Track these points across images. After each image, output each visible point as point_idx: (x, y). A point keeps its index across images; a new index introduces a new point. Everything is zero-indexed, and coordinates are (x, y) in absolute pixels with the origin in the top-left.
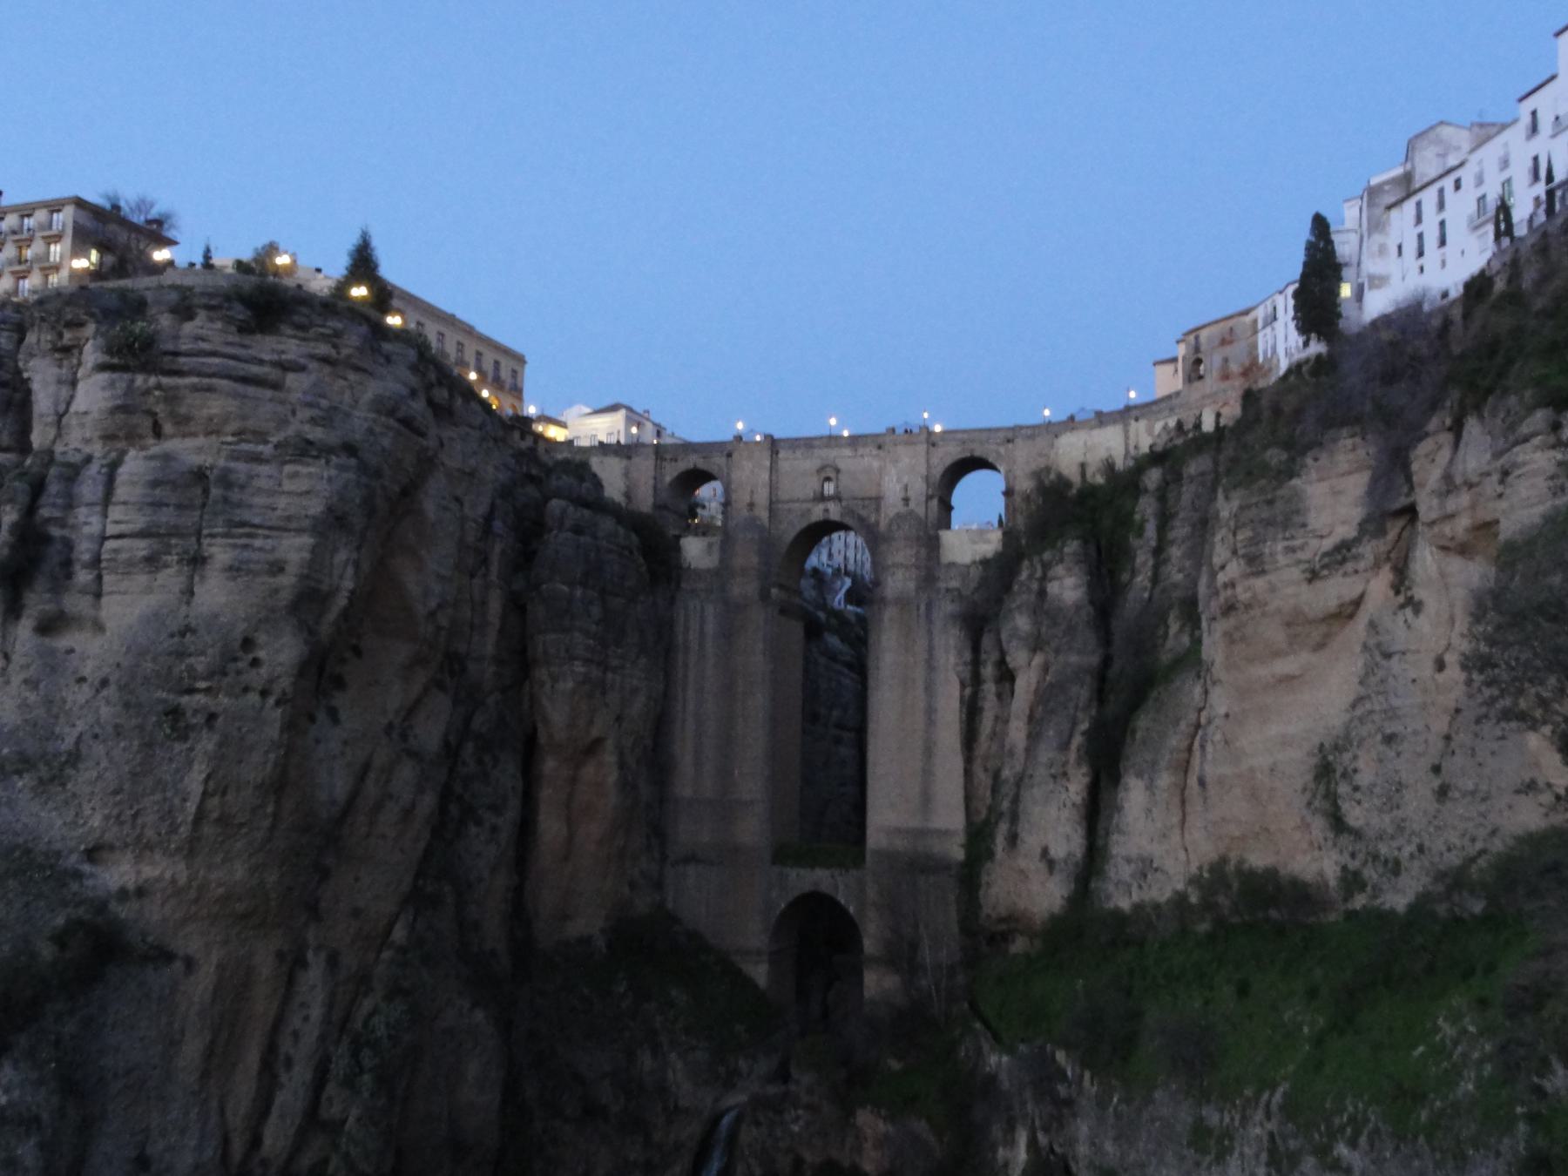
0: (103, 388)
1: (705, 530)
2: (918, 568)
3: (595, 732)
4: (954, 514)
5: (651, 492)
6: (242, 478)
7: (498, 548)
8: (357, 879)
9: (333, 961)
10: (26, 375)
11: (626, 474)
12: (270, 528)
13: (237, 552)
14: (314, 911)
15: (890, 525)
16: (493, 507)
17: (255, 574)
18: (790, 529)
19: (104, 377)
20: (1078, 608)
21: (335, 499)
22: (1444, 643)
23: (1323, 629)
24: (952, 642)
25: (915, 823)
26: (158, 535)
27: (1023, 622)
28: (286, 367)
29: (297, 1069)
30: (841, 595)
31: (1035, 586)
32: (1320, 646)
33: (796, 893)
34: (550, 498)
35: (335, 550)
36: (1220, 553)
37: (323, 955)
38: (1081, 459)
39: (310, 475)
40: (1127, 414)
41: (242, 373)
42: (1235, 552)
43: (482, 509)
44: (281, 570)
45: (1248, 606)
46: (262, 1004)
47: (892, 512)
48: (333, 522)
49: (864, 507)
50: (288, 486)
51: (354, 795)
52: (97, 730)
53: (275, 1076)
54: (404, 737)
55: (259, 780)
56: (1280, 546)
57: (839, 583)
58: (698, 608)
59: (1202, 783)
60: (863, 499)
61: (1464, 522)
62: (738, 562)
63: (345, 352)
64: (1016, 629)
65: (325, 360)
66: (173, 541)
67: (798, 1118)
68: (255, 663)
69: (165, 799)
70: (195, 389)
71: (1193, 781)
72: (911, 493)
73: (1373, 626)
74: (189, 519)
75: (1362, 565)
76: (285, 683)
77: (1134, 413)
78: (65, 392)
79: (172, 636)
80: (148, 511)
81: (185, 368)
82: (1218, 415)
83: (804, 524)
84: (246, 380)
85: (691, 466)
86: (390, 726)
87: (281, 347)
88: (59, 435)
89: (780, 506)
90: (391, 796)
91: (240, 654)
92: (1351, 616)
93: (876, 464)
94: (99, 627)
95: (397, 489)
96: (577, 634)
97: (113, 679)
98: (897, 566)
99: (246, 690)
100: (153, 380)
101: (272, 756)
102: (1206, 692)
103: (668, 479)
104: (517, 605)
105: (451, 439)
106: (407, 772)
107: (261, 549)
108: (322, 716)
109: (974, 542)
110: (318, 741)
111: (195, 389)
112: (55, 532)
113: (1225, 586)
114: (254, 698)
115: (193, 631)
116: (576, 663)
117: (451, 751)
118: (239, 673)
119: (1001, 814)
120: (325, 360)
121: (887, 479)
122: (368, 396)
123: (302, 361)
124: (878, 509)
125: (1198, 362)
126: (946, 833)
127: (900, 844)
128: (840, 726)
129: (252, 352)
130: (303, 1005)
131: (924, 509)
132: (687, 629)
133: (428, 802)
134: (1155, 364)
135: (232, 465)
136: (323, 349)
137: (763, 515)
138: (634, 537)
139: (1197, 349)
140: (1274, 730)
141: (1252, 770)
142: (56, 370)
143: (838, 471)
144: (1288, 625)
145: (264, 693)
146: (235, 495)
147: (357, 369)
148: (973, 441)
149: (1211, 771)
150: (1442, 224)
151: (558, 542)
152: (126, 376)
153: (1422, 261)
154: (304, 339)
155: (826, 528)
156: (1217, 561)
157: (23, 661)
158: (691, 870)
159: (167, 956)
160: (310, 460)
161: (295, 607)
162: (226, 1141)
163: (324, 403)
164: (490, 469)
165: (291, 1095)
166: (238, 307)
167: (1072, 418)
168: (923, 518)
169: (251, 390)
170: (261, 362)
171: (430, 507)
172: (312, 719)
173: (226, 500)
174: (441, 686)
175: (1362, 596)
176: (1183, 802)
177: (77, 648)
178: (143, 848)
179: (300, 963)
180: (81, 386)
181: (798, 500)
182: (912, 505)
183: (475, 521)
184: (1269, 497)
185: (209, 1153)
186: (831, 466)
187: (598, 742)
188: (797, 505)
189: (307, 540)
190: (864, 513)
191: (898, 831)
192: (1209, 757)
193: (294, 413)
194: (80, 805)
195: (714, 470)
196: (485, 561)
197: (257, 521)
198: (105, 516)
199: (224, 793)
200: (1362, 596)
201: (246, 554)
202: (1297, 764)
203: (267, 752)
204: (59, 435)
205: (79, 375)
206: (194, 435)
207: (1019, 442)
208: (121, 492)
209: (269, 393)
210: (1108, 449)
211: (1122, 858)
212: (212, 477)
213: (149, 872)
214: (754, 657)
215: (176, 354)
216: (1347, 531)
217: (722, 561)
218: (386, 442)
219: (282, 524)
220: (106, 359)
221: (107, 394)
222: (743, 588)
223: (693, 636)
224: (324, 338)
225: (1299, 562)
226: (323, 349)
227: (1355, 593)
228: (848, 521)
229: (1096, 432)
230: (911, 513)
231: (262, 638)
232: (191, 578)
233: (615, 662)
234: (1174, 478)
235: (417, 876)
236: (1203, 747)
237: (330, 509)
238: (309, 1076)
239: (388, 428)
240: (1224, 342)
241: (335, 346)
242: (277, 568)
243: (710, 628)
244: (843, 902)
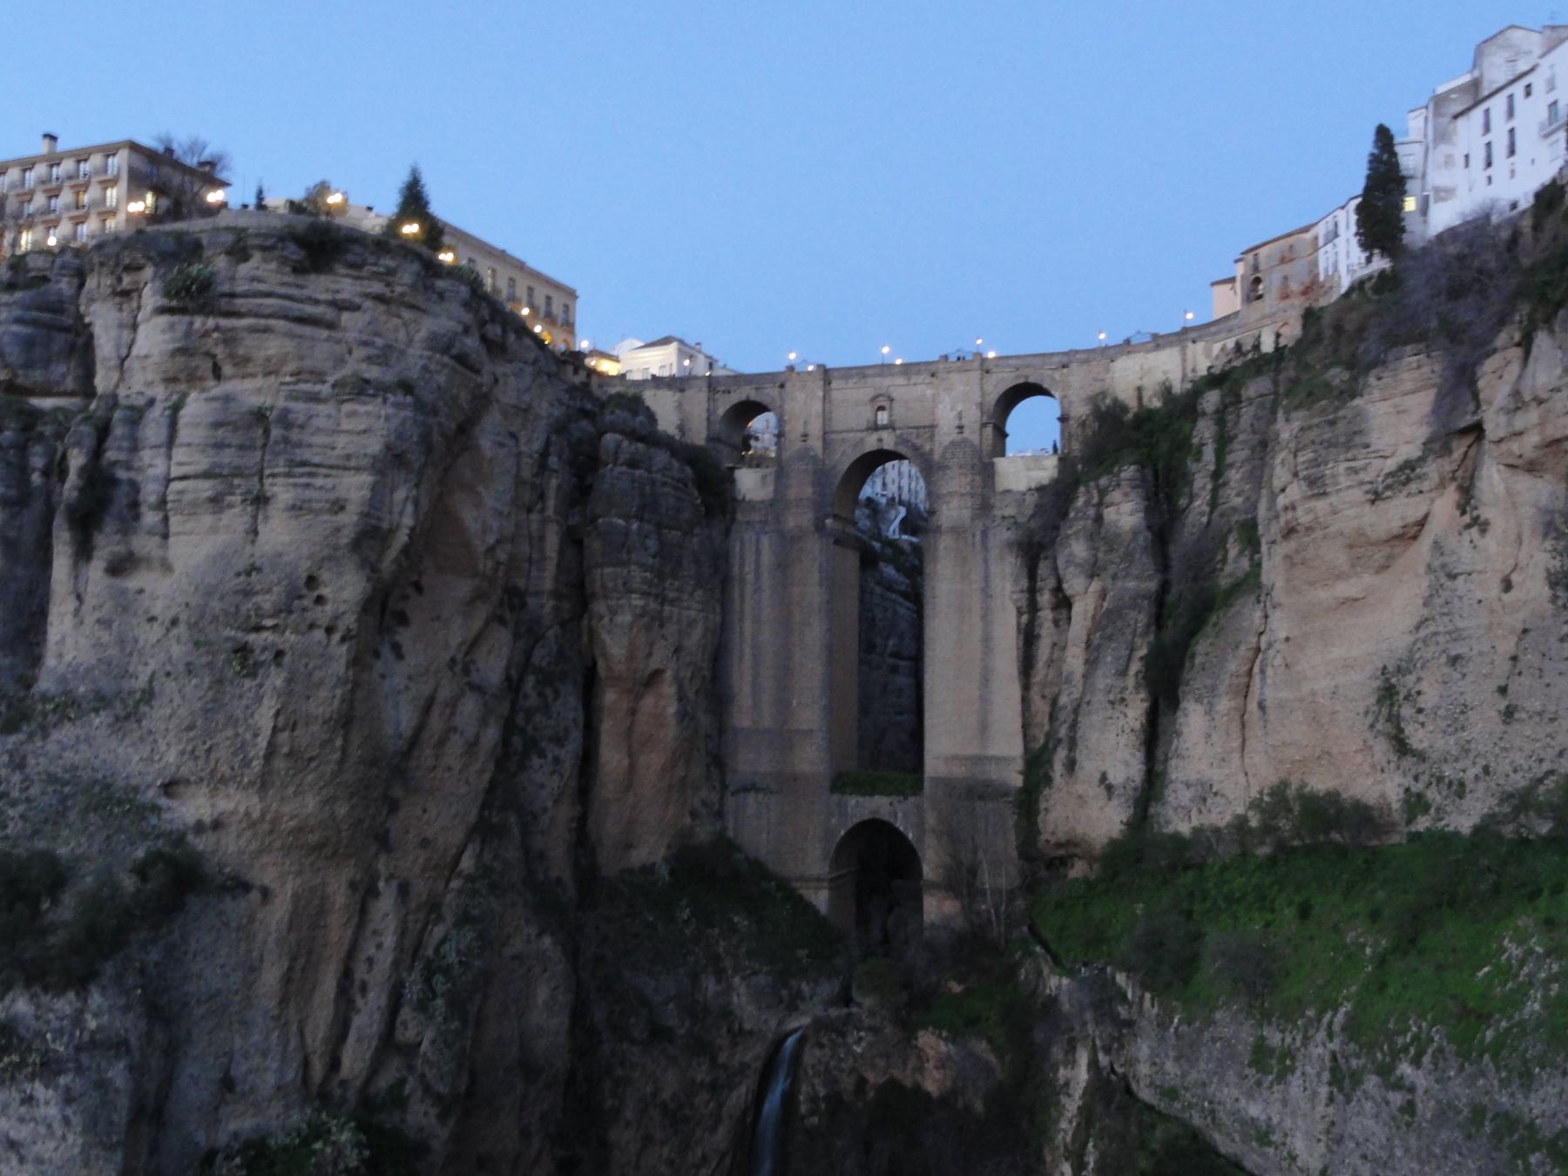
0: (164, 331)
1: (758, 462)
2: (972, 495)
3: (655, 663)
4: (1008, 440)
5: (705, 423)
6: (301, 419)
7: (554, 482)
8: (425, 811)
9: (404, 890)
10: (87, 320)
11: (680, 406)
12: (331, 467)
13: (300, 490)
14: (383, 841)
15: (944, 454)
16: (548, 443)
17: (317, 512)
18: (844, 459)
19: (164, 320)
20: (1135, 533)
21: (392, 438)
22: (1511, 562)
23: (1386, 550)
24: (1008, 570)
25: (972, 750)
26: (220, 476)
27: (1079, 549)
28: (341, 306)
29: (371, 995)
30: (896, 523)
31: (1091, 512)
32: (1384, 568)
33: (856, 821)
34: (606, 432)
35: (393, 490)
36: (1280, 475)
37: (394, 883)
38: (1138, 383)
39: (368, 414)
40: (1185, 336)
41: (297, 313)
42: (1296, 475)
43: (537, 445)
44: (342, 508)
45: (1309, 529)
46: (337, 930)
47: (947, 441)
48: (392, 460)
49: (918, 436)
50: (345, 426)
51: (421, 727)
52: (169, 668)
53: (351, 1002)
54: (466, 671)
55: (327, 715)
56: (1343, 466)
57: (893, 513)
58: (754, 538)
59: (1262, 707)
60: (917, 428)
61: (1533, 439)
62: (792, 493)
63: (399, 289)
64: (1071, 554)
65: (379, 298)
66: (236, 481)
67: (860, 1039)
68: (320, 600)
69: (237, 735)
70: (253, 330)
71: (1253, 706)
72: (964, 422)
73: (1437, 546)
74: (253, 458)
75: (1426, 486)
76: (350, 620)
77: (1193, 335)
78: (126, 335)
79: (238, 574)
80: (211, 452)
81: (243, 310)
82: (1278, 336)
84: (301, 320)
85: (743, 397)
86: (453, 660)
87: (333, 286)
88: (121, 379)
89: (833, 436)
90: (455, 729)
91: (304, 591)
92: (1415, 537)
93: (929, 392)
94: (167, 567)
95: (453, 426)
96: (633, 567)
97: (183, 617)
98: (950, 494)
99: (312, 626)
100: (211, 322)
101: (339, 692)
102: (1266, 617)
103: (721, 411)
104: (574, 540)
105: (505, 375)
106: (470, 706)
107: (321, 488)
108: (386, 651)
109: (1029, 469)
110: (383, 676)
111: (253, 330)
112: (122, 474)
113: (1286, 508)
114: (319, 634)
115: (259, 570)
116: (634, 596)
117: (513, 686)
118: (304, 610)
119: (1059, 741)
120: (379, 298)
121: (940, 406)
122: (423, 334)
123: (358, 300)
124: (932, 438)
125: (1257, 281)
126: (1005, 760)
127: (959, 771)
128: (896, 655)
129: (306, 292)
130: (375, 933)
132: (742, 558)
133: (491, 735)
134: (1213, 284)
135: (292, 405)
136: (377, 287)
137: (816, 444)
138: (689, 470)
139: (1256, 268)
140: (1337, 652)
141: (1313, 693)
142: (118, 314)
143: (891, 400)
144: (1351, 547)
145: (330, 630)
146: (295, 435)
147: (412, 307)
148: (1028, 366)
149: (1271, 696)
150: (1512, 131)
151: (613, 477)
152: (187, 319)
153: (1490, 171)
154: (357, 278)
155: (880, 457)
156: (1277, 484)
157: (94, 601)
158: (751, 798)
159: (246, 887)
160: (368, 399)
161: (356, 545)
162: (306, 1064)
163: (379, 342)
164: (545, 404)
165: (367, 1018)
166: (292, 247)
167: (1127, 342)
168: (976, 442)
169: (308, 330)
170: (317, 302)
171: (486, 443)
172: (377, 654)
173: (286, 440)
174: (501, 620)
175: (1426, 517)
176: (1243, 725)
177: (148, 590)
178: (218, 782)
179: (372, 892)
180: (142, 330)
182: (967, 433)
183: (531, 457)
184: (1331, 417)
185: (290, 1075)
186: (880, 395)
187: (658, 673)
188: (851, 435)
189: (367, 478)
190: (918, 442)
191: (955, 758)
192: (1269, 681)
193: (350, 352)
194: (155, 741)
195: (764, 399)
196: (542, 497)
197: (316, 460)
198: (169, 457)
199: (293, 729)
200: (1426, 517)
201: (309, 494)
202: (1361, 687)
203: (334, 687)
204: (121, 379)
205: (140, 317)
206: (253, 375)
207: (1074, 366)
208: (184, 434)
209: (325, 333)
210: (1165, 372)
212: (272, 416)
213: (224, 805)
214: (811, 590)
215: (233, 295)
216: (1412, 451)
217: (776, 491)
218: (441, 379)
219: (341, 462)
220: (164, 302)
221: (167, 337)
222: (799, 519)
223: (749, 567)
224: (375, 276)
225: (1362, 483)
226: (377, 287)
227: (1419, 514)
228: (902, 450)
229: (1152, 356)
230: (965, 441)
231: (325, 575)
232: (255, 517)
233: (671, 595)
234: (1233, 400)
235: (484, 806)
236: (1263, 672)
237: (388, 447)
238: (383, 1001)
239: (444, 365)
240: (1283, 261)
241: (388, 285)
242: (338, 506)
243: (767, 558)
244: (901, 829)
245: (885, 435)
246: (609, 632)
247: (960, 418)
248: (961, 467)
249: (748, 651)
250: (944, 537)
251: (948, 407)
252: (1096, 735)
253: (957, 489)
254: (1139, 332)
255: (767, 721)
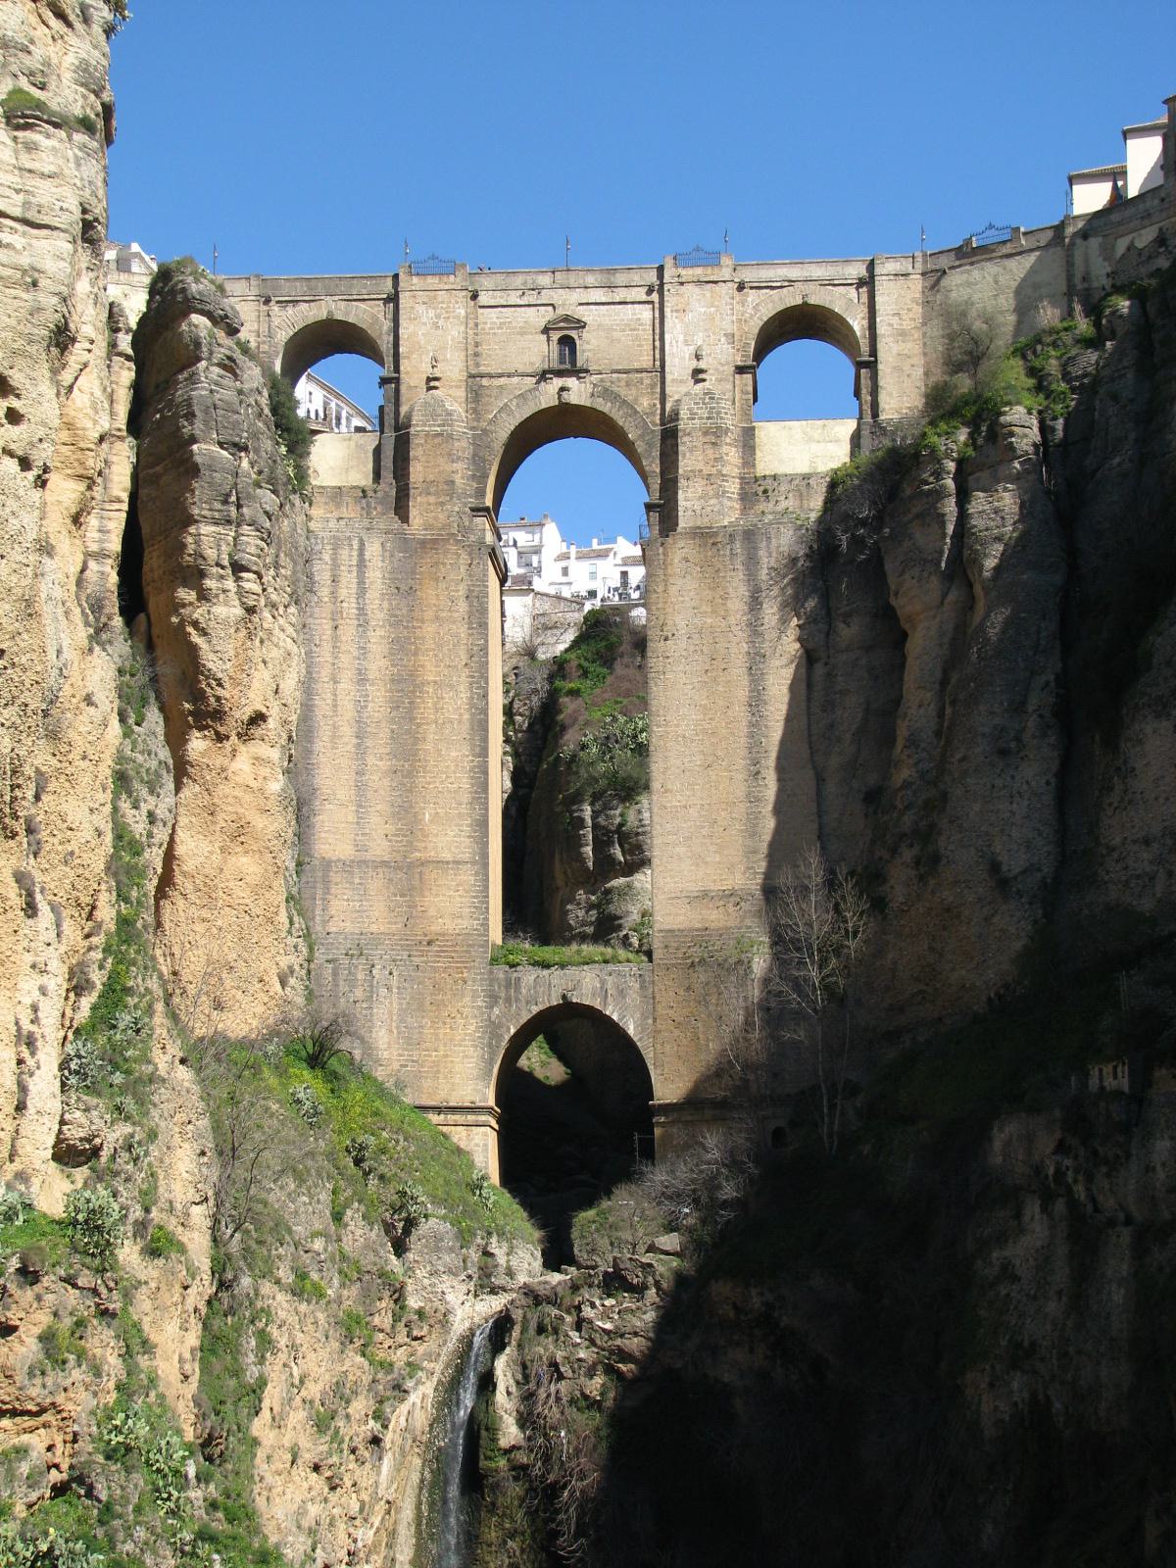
33: (535, 1009)
49: (628, 385)
60: (626, 372)
62: (417, 472)
83: (527, 413)
85: (323, 315)
103: (283, 336)
116: (244, 575)
131: (730, 386)
137: (453, 399)
143: (581, 325)
181: (516, 374)
182: (711, 382)
186: (567, 319)
188: (515, 380)
190: (629, 395)
191: (705, 895)
211: (1135, 842)
243: (376, 575)
244: (615, 1017)
245: (571, 382)
246: (204, 633)
247: (698, 357)
248: (706, 433)
249: (347, 731)
250: (681, 544)
251: (681, 338)
252: (977, 807)
253: (700, 466)
254: (991, 227)
255: (380, 849)
